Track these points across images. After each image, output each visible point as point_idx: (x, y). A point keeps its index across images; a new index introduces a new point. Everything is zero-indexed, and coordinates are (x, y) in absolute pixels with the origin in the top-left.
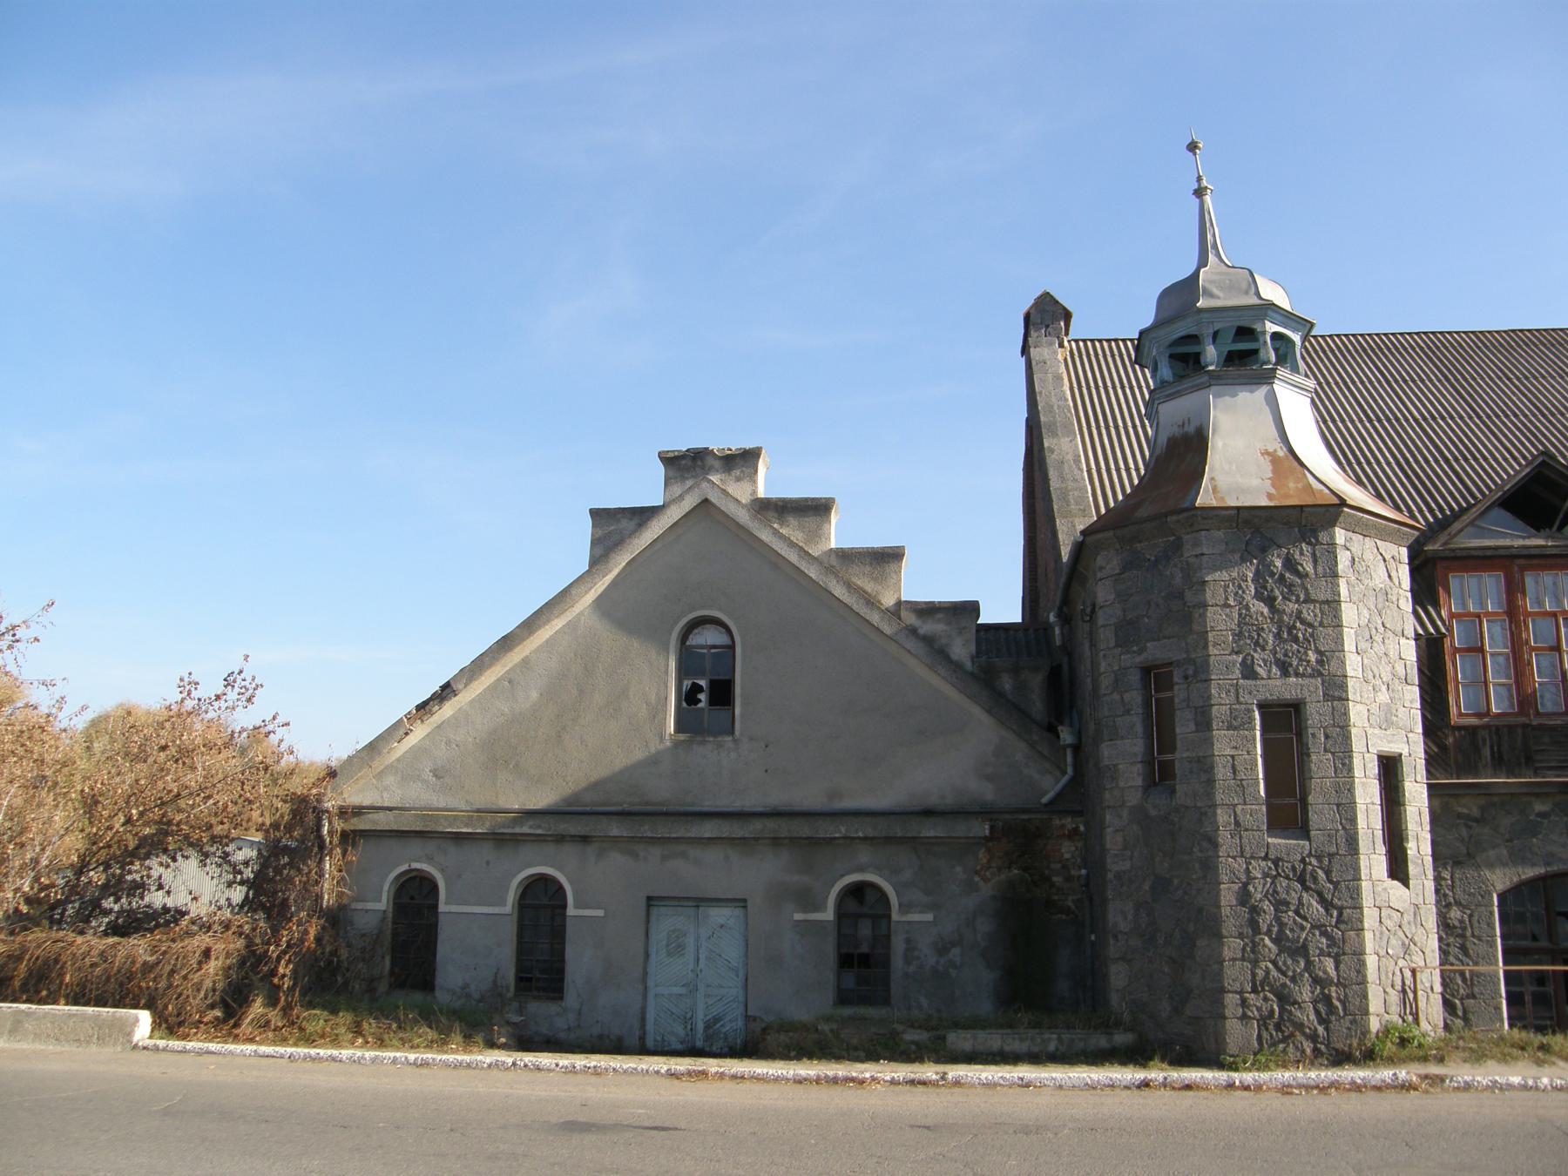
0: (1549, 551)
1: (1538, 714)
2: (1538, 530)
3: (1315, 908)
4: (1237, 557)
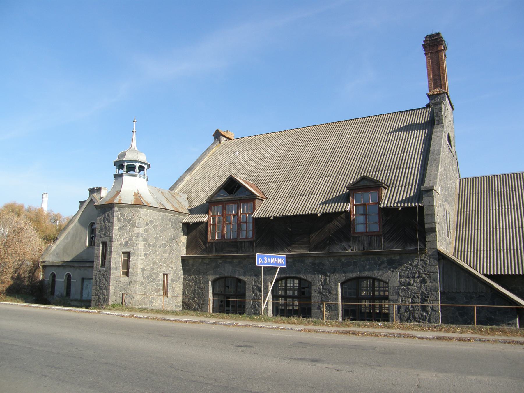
0: (230, 200)
1: (225, 239)
2: (230, 194)
3: (104, 281)
4: (102, 214)
